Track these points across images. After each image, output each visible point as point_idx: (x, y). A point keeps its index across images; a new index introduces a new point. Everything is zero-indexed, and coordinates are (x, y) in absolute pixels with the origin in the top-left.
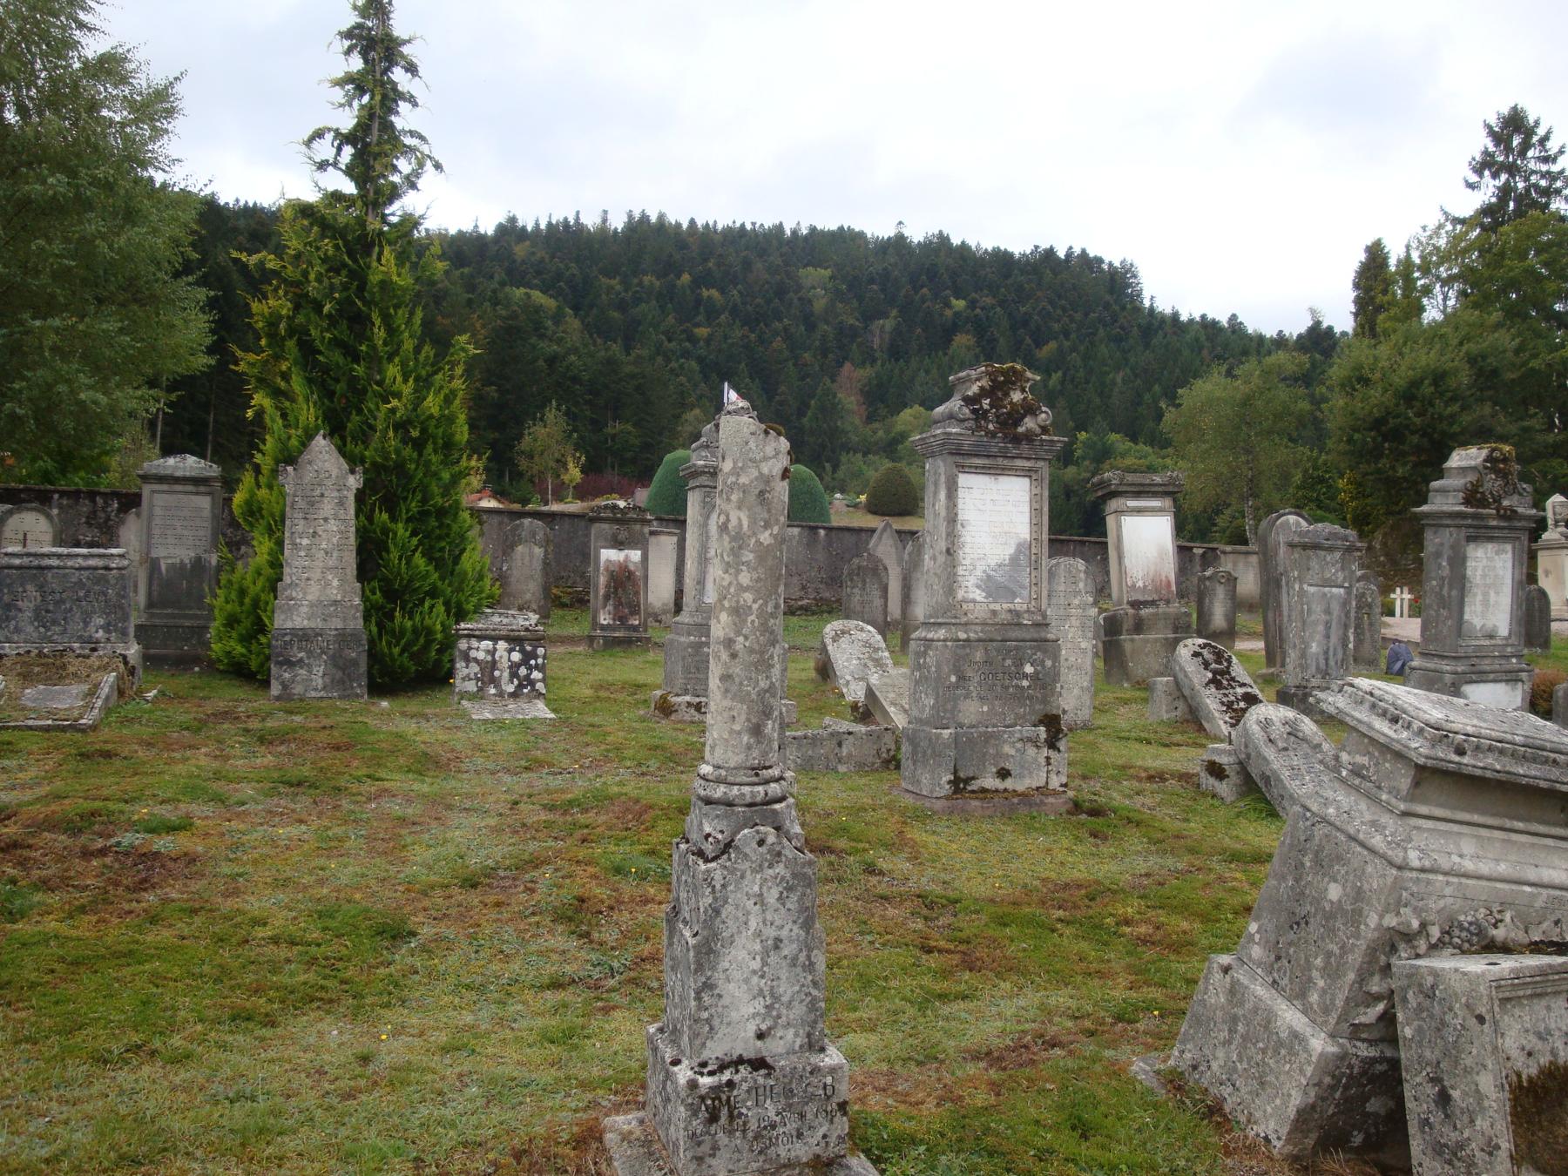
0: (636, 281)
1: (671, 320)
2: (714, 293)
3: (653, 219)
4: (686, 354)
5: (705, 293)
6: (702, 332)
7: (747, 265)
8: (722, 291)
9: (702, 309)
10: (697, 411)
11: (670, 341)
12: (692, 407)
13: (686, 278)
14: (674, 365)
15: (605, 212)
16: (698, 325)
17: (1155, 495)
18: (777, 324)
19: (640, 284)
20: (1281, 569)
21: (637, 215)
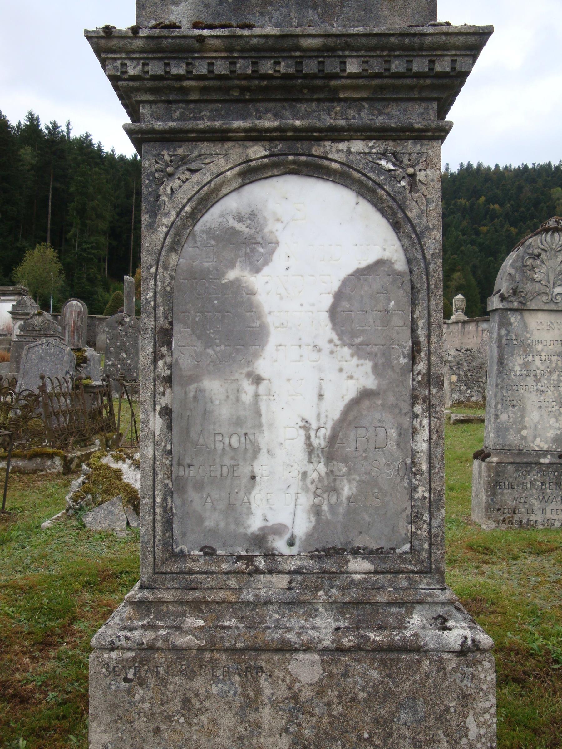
0: (453, 202)
1: (465, 223)
2: (497, 206)
3: (475, 166)
4: (473, 243)
5: (492, 207)
6: (484, 229)
7: (520, 188)
8: (502, 205)
9: (488, 217)
10: (459, 273)
11: (463, 235)
12: (459, 271)
13: (482, 199)
14: (463, 248)
15: (448, 164)
16: (484, 225)
17: (11, 294)
18: (528, 222)
19: (455, 204)
20: (67, 322)
21: (465, 165)
